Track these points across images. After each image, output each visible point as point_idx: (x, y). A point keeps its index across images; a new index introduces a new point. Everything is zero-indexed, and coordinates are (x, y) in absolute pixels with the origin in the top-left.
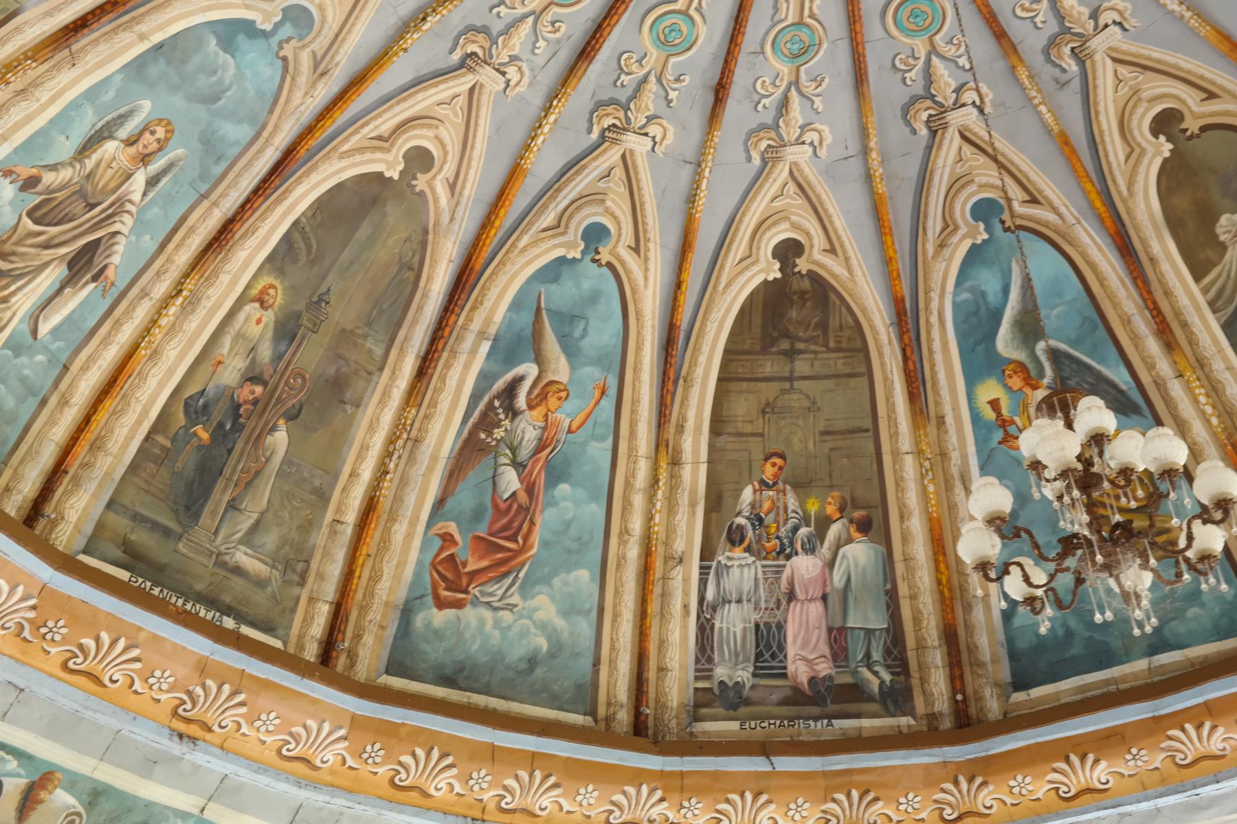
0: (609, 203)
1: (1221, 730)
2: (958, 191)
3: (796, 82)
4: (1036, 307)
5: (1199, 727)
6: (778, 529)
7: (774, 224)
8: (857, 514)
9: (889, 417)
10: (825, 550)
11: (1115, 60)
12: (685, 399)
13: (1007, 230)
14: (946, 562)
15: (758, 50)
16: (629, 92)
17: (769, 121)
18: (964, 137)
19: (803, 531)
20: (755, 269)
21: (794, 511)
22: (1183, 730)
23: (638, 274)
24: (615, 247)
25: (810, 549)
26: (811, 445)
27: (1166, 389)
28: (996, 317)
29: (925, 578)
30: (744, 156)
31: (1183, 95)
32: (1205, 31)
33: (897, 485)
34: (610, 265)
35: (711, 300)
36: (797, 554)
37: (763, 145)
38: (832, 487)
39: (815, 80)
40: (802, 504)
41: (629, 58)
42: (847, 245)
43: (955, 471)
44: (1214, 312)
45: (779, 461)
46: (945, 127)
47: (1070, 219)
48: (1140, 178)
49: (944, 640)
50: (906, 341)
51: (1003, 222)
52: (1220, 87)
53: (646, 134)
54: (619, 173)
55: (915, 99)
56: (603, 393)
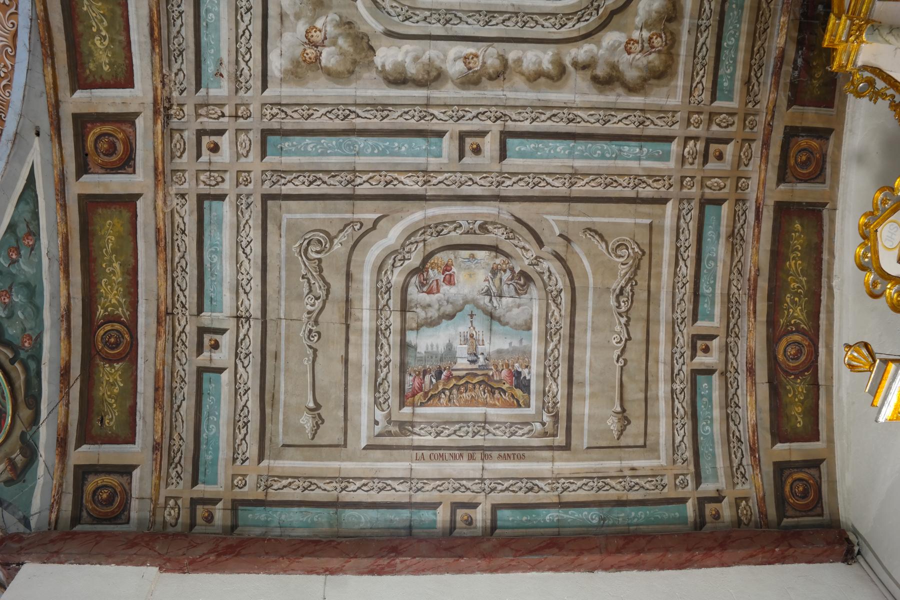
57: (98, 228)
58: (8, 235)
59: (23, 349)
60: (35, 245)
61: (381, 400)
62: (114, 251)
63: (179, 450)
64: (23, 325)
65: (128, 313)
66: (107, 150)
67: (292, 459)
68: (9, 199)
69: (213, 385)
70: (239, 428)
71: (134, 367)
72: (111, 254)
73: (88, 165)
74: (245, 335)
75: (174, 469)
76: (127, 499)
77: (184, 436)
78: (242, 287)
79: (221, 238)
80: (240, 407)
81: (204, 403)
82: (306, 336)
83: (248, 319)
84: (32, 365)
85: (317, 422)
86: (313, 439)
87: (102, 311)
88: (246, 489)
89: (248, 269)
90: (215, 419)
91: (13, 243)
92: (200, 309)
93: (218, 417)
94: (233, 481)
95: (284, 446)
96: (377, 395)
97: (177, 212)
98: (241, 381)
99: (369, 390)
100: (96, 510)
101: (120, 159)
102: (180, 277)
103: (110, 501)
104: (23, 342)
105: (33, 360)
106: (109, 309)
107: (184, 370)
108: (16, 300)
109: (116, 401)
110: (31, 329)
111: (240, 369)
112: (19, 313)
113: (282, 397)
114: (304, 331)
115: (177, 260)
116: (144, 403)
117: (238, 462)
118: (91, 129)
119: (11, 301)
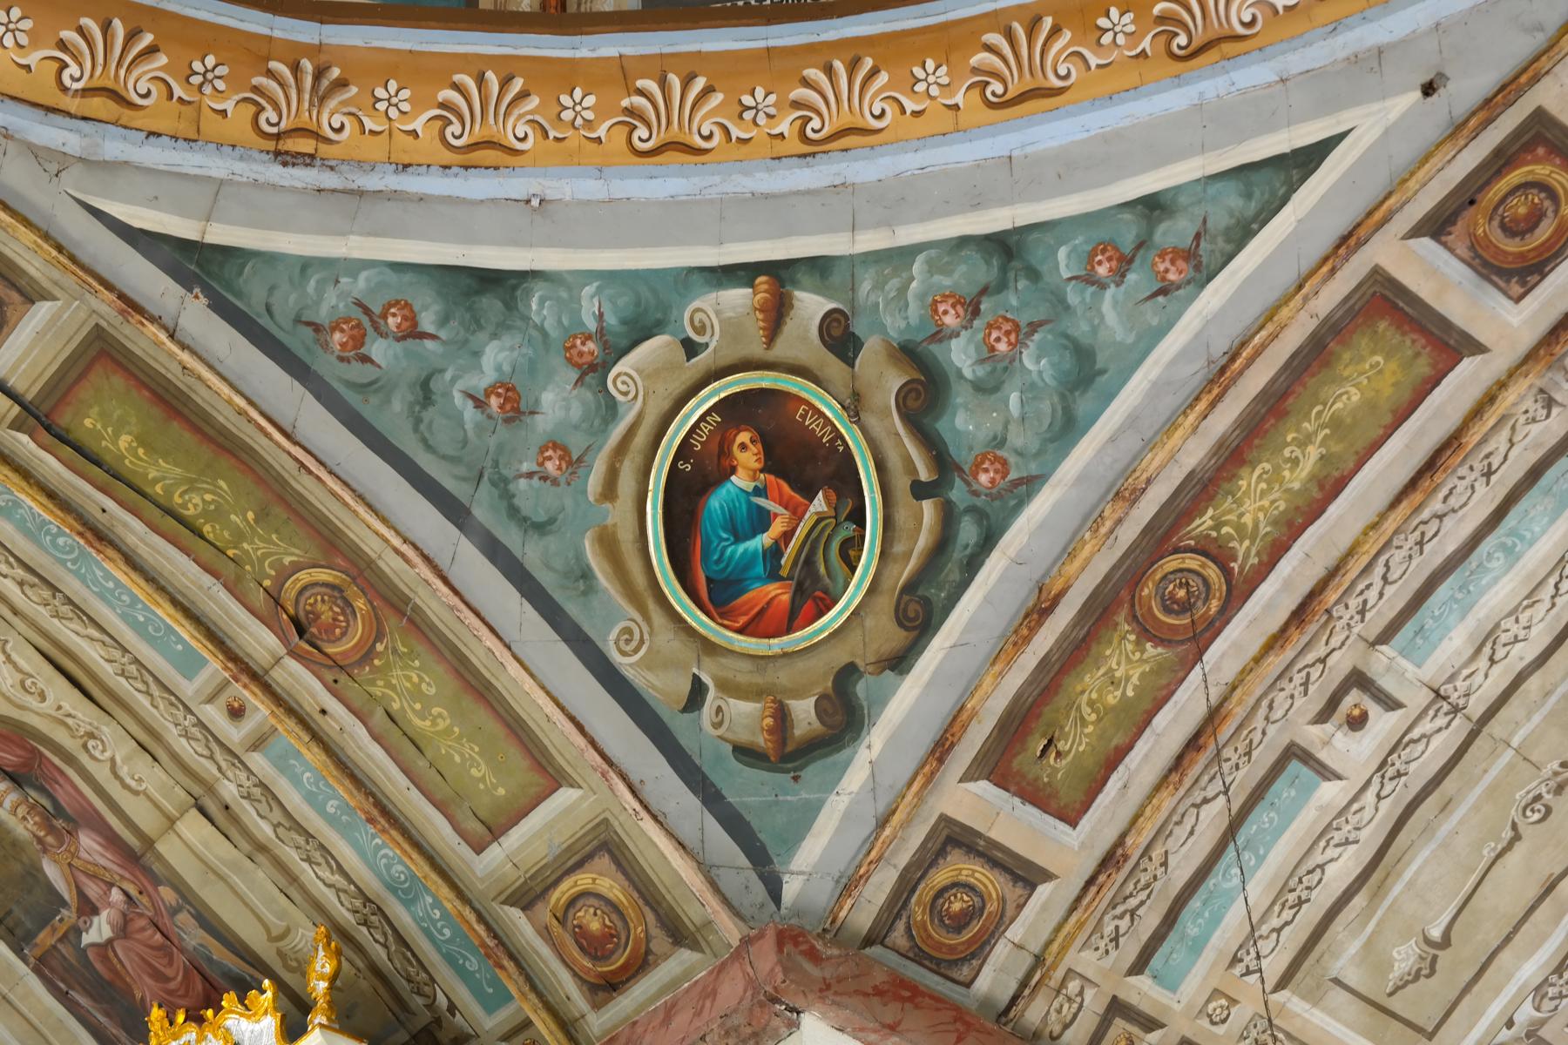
57: (1347, 356)
58: (1127, 216)
59: (968, 484)
60: (1179, 288)
61: (1552, 991)
62: (1336, 424)
63: (1147, 886)
64: (1006, 427)
65: (1256, 561)
66: (1515, 220)
67: (1331, 1013)
68: (1203, 149)
69: (1293, 793)
70: (1283, 905)
71: (1181, 674)
72: (1323, 426)
73: (1454, 223)
74: (1423, 736)
75: (1115, 917)
76: (993, 933)
77: (1172, 861)
78: (1494, 643)
79: (1544, 532)
80: (1310, 864)
81: (1252, 817)
82: (1523, 804)
83: (1456, 710)
84: (968, 532)
85: (1419, 970)
86: (1391, 994)
87: (1210, 523)
88: (1220, 1030)
89: (1535, 621)
90: (1252, 863)
91: (1127, 241)
92: (1385, 636)
93: (1261, 859)
94: (1208, 1001)
95: (1337, 981)
96: (1554, 978)
97: (1513, 428)
98: (1353, 819)
99: (1547, 962)
100: (926, 930)
101: (1522, 256)
102: (1404, 552)
103: (960, 922)
104: (977, 467)
105: (979, 523)
106: (1225, 530)
107: (1264, 733)
108: (1028, 362)
109: (1099, 720)
111: (1370, 796)
112: (1014, 399)
113: (1397, 889)
114: (1528, 792)
115: (1425, 515)
116: (1146, 755)
117: (1239, 969)
118: (1537, 161)
119: (1013, 359)
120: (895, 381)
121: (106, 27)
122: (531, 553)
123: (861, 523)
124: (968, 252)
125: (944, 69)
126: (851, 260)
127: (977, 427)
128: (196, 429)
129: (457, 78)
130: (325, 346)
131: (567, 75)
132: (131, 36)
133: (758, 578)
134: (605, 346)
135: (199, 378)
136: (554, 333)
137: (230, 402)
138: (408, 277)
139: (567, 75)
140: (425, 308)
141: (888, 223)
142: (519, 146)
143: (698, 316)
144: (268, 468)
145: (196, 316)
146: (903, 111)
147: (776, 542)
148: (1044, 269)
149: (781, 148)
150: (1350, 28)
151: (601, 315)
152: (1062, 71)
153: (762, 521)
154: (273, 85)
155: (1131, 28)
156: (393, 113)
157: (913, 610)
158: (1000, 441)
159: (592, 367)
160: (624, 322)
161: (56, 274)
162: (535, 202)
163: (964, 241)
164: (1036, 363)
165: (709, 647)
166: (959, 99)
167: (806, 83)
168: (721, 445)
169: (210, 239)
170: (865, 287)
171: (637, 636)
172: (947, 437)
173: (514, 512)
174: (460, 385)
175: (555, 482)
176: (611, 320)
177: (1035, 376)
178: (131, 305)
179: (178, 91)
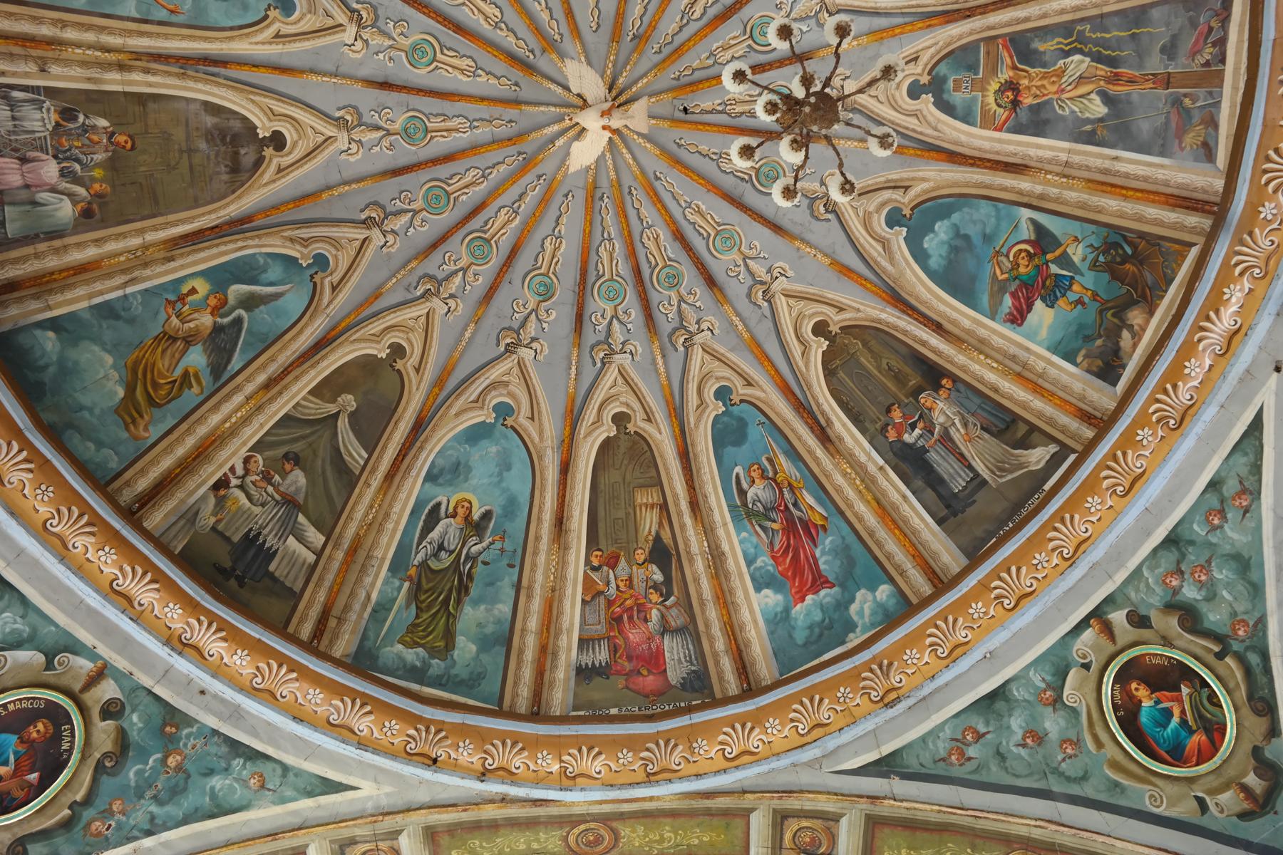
0: (309, 16)
1: (30, 476)
2: (330, 243)
3: (389, 133)
4: (265, 304)
5: (26, 460)
6: (77, 147)
7: (296, 130)
8: (95, 206)
9: (168, 223)
10: (65, 185)
11: (428, 313)
12: (168, 74)
13: (312, 277)
14: (68, 277)
15: (410, 107)
16: (383, 27)
17: (364, 120)
18: (365, 240)
19: (77, 167)
20: (265, 119)
21: (92, 159)
22: (20, 451)
23: (260, 37)
24: (279, 21)
25: (64, 173)
26: (143, 169)
27: (236, 393)
28: (253, 281)
29: (52, 262)
30: (341, 105)
31: (414, 356)
32: (457, 354)
33: (120, 235)
34: (266, 17)
35: (242, 91)
36: (58, 163)
37: (348, 117)
38: (113, 187)
39: (391, 145)
40: (97, 165)
41: (404, 27)
42: (284, 180)
43: (136, 273)
44: (294, 407)
45: (129, 146)
46: (369, 228)
47: (328, 311)
48: (363, 345)
49: (5, 282)
50: (206, 233)
51: (316, 273)
52: (423, 373)
53: (356, 40)
54: (330, 22)
55: (383, 208)
56: (172, 12)
58: (1208, 496)
64: (1231, 605)
68: (1214, 451)
84: (1254, 659)
91: (1214, 502)
104: (1234, 630)
105: (1255, 652)
108: (1220, 577)
110: (1246, 613)
112: (1225, 593)
119: (1211, 579)
120: (1173, 621)
121: (802, 704)
122: (1088, 791)
123: (1208, 686)
124: (1161, 553)
125: (1096, 497)
126: (1119, 589)
127: (1220, 615)
128: (926, 830)
129: (928, 632)
130: (952, 764)
131: (964, 603)
132: (812, 700)
133: (1186, 738)
134: (1054, 689)
135: (915, 809)
136: (1031, 699)
137: (932, 810)
138: (963, 717)
139: (964, 603)
140: (977, 724)
141: (1122, 565)
142: (967, 640)
143: (1080, 652)
144: (962, 827)
145: (899, 786)
146: (1093, 523)
147: (1181, 718)
148: (1194, 537)
149: (1060, 569)
150: (1229, 372)
151: (1043, 679)
152: (1139, 465)
153: (1168, 714)
154: (868, 682)
155: (1151, 432)
156: (915, 661)
157: (1260, 706)
158: (1234, 614)
159: (1055, 701)
160: (1054, 675)
161: (840, 805)
162: (988, 655)
163: (1155, 551)
164: (1222, 574)
165: (1190, 780)
166: (1110, 503)
167: (1051, 540)
168: (1128, 695)
169: (884, 754)
170: (1133, 595)
171: (1157, 796)
172: (1212, 627)
173: (1069, 779)
174: (1011, 744)
175: (1076, 756)
176: (1048, 678)
177: (1226, 579)
178: (873, 798)
179: (839, 708)
